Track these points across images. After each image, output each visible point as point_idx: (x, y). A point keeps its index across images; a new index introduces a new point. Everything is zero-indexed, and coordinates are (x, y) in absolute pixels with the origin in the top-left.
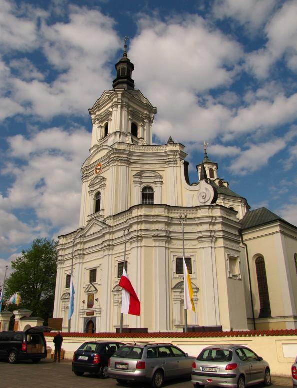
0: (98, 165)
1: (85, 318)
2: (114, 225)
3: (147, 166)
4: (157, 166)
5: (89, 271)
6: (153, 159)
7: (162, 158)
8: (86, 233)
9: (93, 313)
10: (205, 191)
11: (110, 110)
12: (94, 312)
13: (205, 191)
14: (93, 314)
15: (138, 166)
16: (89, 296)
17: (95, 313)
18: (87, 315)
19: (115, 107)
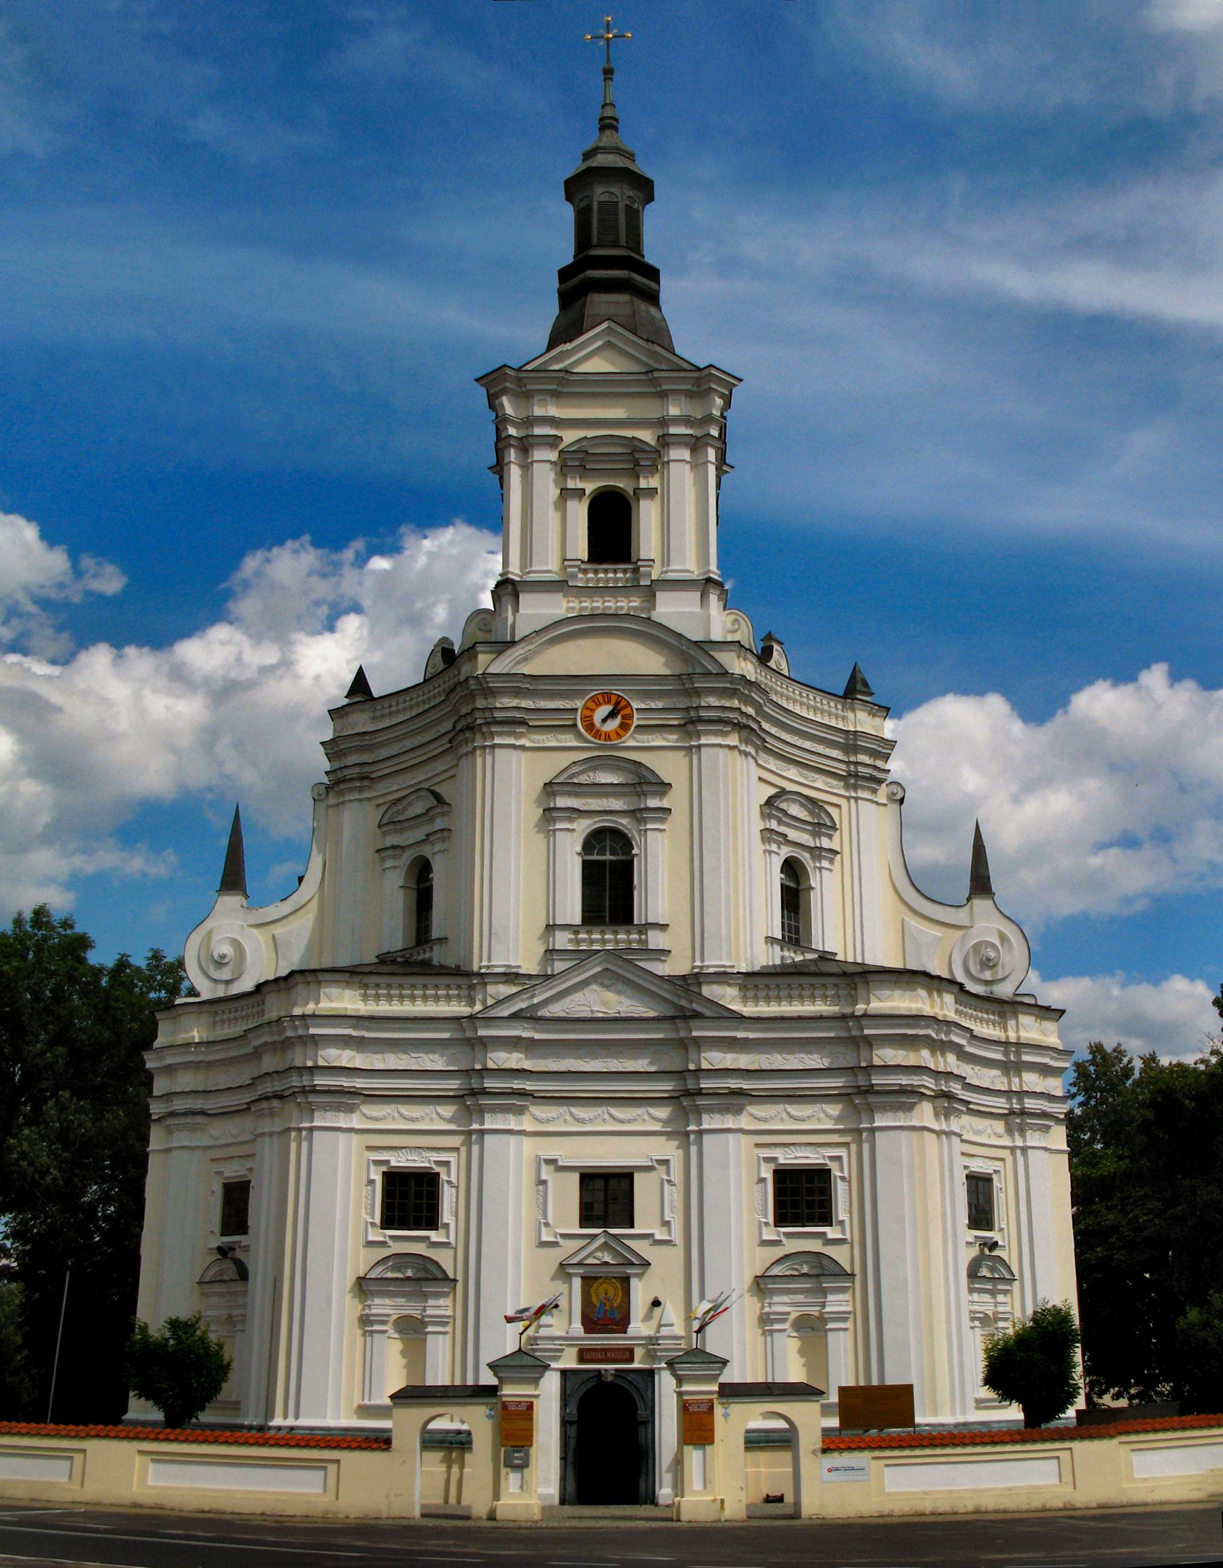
0: (606, 697)
1: (564, 1373)
2: (749, 1010)
3: (792, 772)
4: (820, 782)
5: (575, 1178)
6: (807, 745)
7: (835, 753)
8: (545, 1003)
9: (628, 1354)
10: (998, 943)
11: (647, 436)
12: (631, 1351)
13: (998, 943)
14: (631, 1360)
15: (773, 764)
16: (587, 1281)
17: (639, 1353)
18: (582, 1358)
19: (686, 445)
